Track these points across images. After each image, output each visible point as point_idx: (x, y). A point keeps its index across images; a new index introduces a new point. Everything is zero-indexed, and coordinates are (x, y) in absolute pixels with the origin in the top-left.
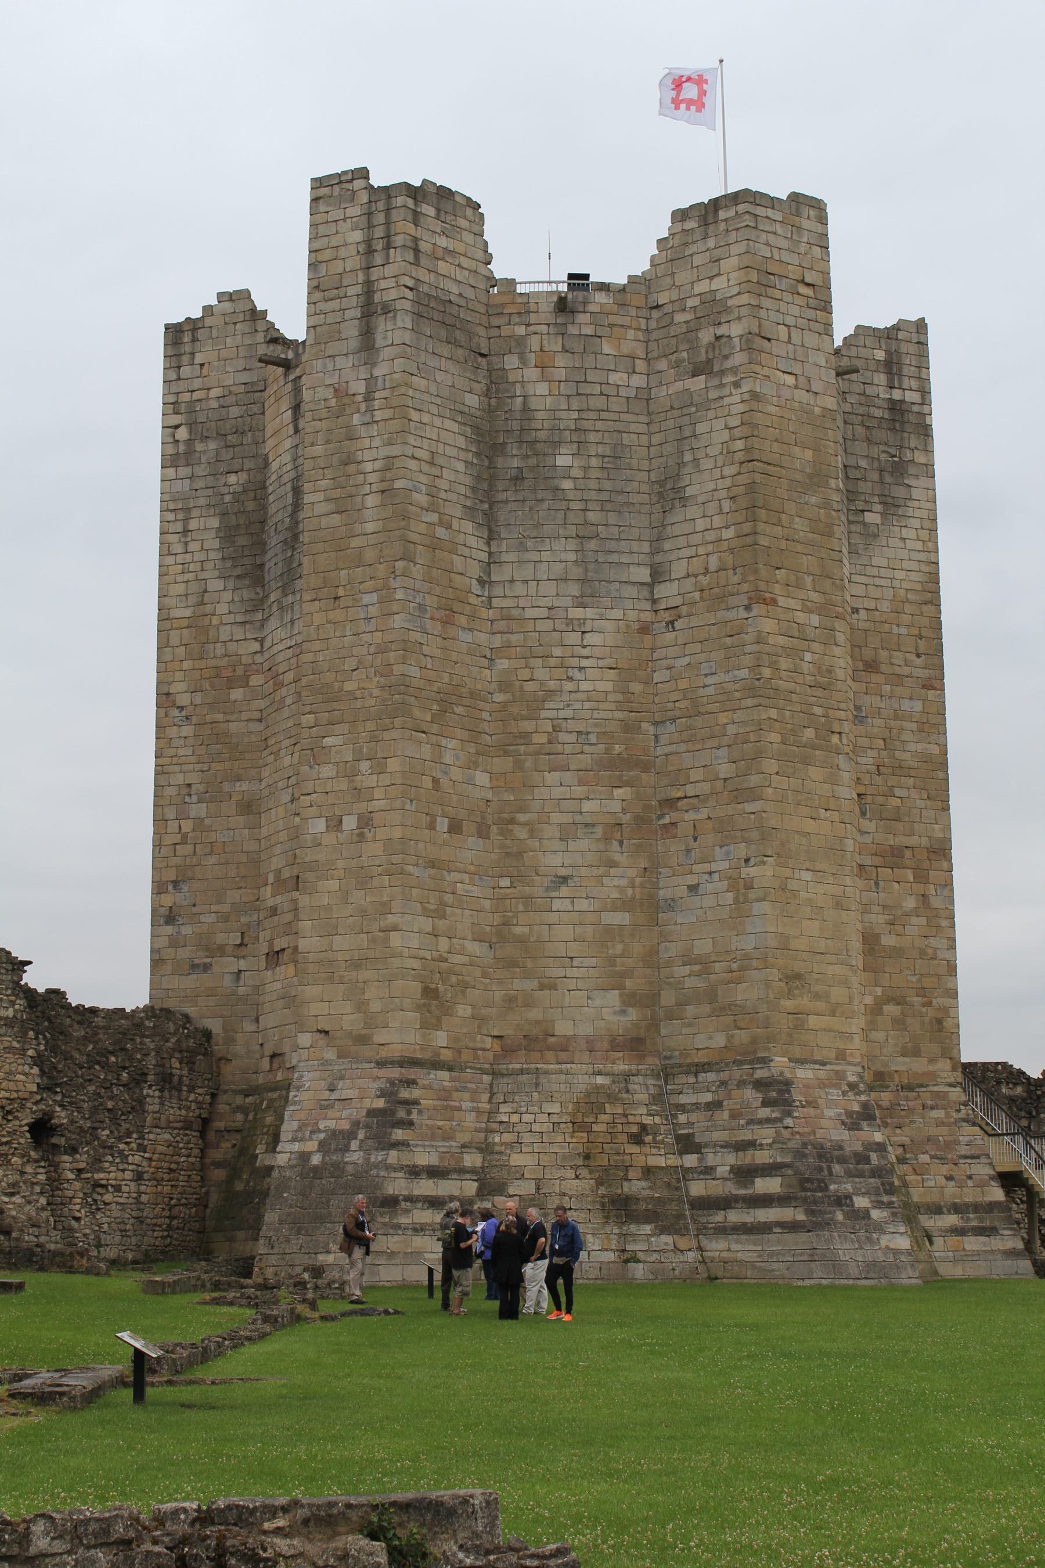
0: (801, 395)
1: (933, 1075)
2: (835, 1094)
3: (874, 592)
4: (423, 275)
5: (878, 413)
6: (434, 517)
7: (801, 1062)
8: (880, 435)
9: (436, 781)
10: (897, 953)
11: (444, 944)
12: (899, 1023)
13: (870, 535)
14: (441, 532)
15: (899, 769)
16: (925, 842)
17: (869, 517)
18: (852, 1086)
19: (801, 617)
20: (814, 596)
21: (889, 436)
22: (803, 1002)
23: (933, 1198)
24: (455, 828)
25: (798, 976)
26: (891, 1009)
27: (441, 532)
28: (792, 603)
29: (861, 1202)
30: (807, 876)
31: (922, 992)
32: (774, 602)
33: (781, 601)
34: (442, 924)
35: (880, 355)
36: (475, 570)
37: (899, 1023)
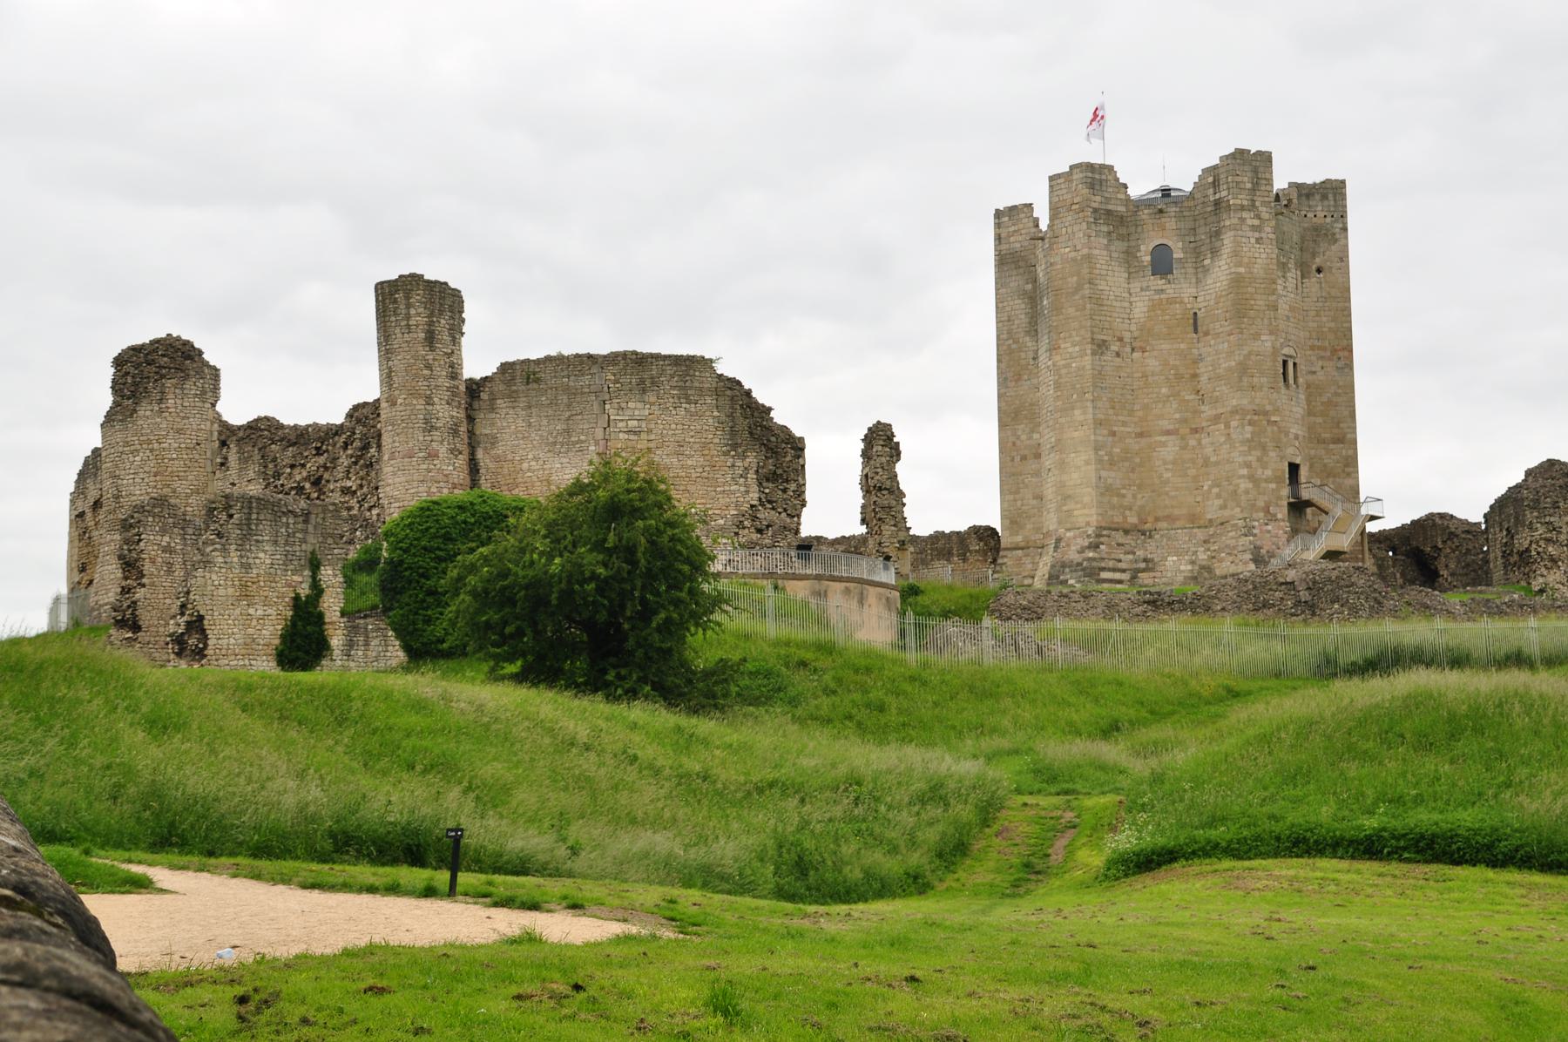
1: (1233, 517)
2: (1079, 541)
4: (1004, 247)
7: (1068, 530)
8: (1210, 219)
10: (1217, 463)
12: (1218, 496)
13: (1206, 270)
15: (1219, 378)
17: (1207, 262)
21: (1213, 218)
22: (1070, 505)
23: (1224, 572)
24: (1024, 458)
26: (1215, 490)
29: (1071, 582)
31: (1228, 479)
35: (1211, 179)
36: (1031, 355)
37: (1218, 496)
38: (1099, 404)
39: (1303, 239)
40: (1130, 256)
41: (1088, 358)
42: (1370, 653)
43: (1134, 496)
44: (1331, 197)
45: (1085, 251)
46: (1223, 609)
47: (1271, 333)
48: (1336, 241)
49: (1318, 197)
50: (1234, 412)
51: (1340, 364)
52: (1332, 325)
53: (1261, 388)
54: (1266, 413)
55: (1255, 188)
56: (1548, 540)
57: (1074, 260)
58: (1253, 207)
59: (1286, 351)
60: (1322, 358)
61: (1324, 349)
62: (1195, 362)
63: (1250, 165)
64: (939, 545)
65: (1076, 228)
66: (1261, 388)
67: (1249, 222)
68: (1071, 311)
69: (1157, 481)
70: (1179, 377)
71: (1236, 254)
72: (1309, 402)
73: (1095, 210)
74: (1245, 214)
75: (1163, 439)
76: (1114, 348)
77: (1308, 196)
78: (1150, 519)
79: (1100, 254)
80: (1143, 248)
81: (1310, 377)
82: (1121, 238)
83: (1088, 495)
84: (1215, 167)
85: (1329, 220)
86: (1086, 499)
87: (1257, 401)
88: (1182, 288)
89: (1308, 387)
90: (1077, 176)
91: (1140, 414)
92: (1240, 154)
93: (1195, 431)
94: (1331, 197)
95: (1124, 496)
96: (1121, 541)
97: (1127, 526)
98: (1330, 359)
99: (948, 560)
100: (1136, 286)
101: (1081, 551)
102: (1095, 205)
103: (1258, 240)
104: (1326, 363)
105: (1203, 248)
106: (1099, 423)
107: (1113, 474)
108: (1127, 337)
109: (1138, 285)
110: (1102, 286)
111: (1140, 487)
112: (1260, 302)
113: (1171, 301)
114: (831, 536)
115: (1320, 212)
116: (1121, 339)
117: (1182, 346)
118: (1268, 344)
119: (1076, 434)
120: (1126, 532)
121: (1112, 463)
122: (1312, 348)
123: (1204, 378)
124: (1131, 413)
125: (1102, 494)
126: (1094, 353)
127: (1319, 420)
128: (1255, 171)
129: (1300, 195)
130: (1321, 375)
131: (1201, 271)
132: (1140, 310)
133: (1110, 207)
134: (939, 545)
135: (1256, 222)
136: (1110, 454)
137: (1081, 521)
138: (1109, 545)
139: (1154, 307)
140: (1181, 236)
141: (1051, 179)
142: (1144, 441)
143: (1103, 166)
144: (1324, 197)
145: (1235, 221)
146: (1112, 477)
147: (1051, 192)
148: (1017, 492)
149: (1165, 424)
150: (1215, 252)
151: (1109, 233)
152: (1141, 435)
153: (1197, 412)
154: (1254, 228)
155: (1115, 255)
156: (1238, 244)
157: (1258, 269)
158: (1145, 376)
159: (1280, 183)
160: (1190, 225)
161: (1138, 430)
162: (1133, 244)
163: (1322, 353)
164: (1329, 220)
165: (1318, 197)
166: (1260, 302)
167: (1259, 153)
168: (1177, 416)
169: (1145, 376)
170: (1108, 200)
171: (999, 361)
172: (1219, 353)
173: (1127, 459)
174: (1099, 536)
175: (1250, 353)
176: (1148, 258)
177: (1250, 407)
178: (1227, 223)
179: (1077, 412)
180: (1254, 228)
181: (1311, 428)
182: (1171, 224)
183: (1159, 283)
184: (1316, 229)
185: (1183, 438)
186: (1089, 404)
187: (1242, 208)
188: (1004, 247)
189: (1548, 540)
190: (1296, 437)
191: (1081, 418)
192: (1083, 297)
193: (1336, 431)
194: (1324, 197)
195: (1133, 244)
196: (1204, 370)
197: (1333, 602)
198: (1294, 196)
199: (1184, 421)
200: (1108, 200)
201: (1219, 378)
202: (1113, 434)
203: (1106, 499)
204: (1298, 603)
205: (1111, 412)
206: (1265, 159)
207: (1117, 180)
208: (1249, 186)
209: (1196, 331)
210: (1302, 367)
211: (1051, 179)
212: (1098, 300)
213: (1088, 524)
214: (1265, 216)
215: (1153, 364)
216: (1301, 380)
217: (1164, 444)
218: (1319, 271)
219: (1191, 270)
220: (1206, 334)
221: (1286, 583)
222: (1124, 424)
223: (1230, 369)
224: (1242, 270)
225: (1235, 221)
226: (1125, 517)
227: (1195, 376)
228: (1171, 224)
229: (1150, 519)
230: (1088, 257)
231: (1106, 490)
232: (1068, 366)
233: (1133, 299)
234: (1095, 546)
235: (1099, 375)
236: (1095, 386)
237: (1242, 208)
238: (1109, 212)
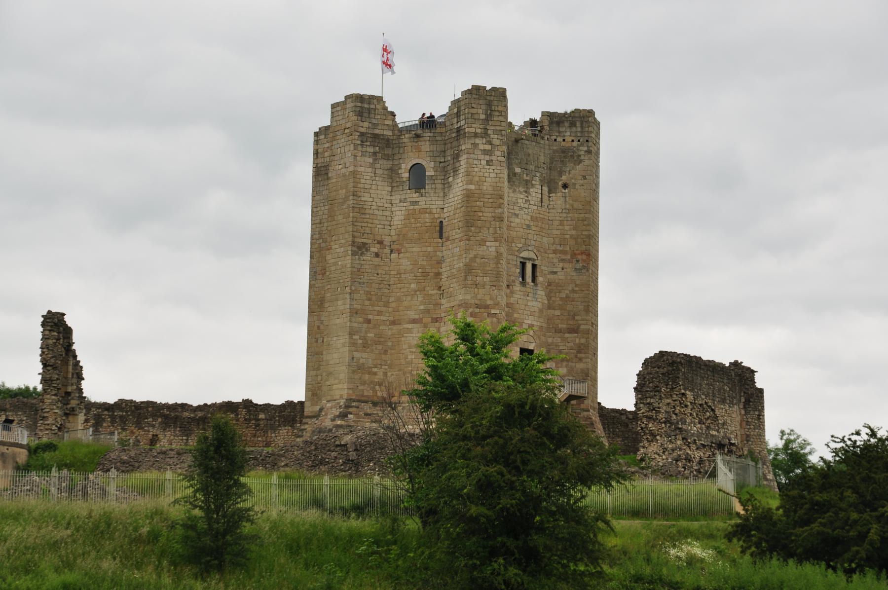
0: (344, 171)
3: (450, 209)
4: (320, 160)
5: (454, 135)
6: (321, 241)
7: (328, 401)
9: (318, 327)
11: (319, 378)
14: (323, 245)
15: (453, 276)
16: (458, 302)
17: (451, 179)
18: (340, 407)
19: (338, 250)
20: (343, 241)
21: (455, 143)
25: (331, 373)
27: (323, 245)
28: (337, 246)
30: (335, 339)
32: (331, 248)
33: (333, 247)
34: (319, 372)
35: (455, 111)
38: (356, 296)
39: (552, 159)
40: (393, 172)
41: (349, 257)
42: (358, 501)
43: (385, 374)
44: (578, 124)
45: (351, 169)
46: (286, 465)
47: (496, 240)
48: (580, 161)
49: (567, 124)
50: (460, 306)
51: (578, 266)
52: (574, 232)
53: (483, 286)
54: (487, 307)
55: (489, 118)
56: (650, 418)
57: (344, 175)
58: (485, 134)
59: (525, 254)
60: (563, 260)
61: (564, 252)
62: (440, 262)
63: (486, 102)
64: (286, 413)
65: (347, 148)
66: (483, 286)
67: (481, 147)
68: (340, 217)
69: (403, 362)
70: (425, 275)
71: (468, 174)
72: (549, 297)
73: (362, 134)
74: (478, 141)
75: (410, 326)
76: (374, 249)
77: (559, 123)
78: (397, 394)
79: (366, 172)
80: (403, 166)
81: (551, 277)
82: (387, 157)
83: (343, 372)
84: (458, 100)
85: (575, 144)
86: (342, 376)
87: (479, 297)
88: (431, 201)
89: (550, 284)
90: (350, 105)
91: (393, 305)
92: (476, 92)
93: (436, 320)
94: (578, 124)
95: (375, 374)
96: (369, 411)
97: (375, 399)
98: (570, 262)
99: (292, 426)
100: (396, 198)
101: (333, 420)
102: (363, 130)
103: (489, 163)
104: (566, 265)
105: (447, 170)
106: (354, 312)
107: (365, 355)
108: (387, 240)
109: (398, 197)
110: (366, 197)
111: (390, 366)
112: (488, 214)
113: (423, 211)
114: (195, 404)
115: (568, 137)
116: (380, 242)
117: (429, 249)
118: (493, 249)
119: (338, 321)
120: (375, 404)
121: (365, 346)
122: (555, 252)
123: (444, 276)
124: (387, 304)
125: (354, 372)
126: (354, 254)
127: (558, 313)
128: (489, 104)
129: (551, 123)
130: (561, 276)
131: (447, 186)
132: (398, 218)
133: (377, 132)
134: (286, 413)
135: (488, 147)
136: (364, 338)
137: (337, 393)
138: (357, 415)
139: (407, 217)
140: (434, 157)
141: (334, 106)
142: (396, 328)
143: (372, 98)
144: (573, 124)
145: (469, 146)
146: (365, 357)
147: (332, 117)
148: (318, 369)
149: (412, 314)
150: (455, 171)
151: (375, 154)
152: (393, 323)
153: (438, 305)
154: (485, 152)
155: (378, 171)
156: (470, 165)
157: (487, 187)
158: (399, 274)
159: (518, 114)
160: (442, 148)
161: (392, 319)
162: (396, 162)
163: (563, 257)
164: (575, 144)
165: (567, 124)
166: (488, 214)
167: (494, 89)
168: (422, 307)
169: (399, 274)
170: (375, 126)
171: (312, 257)
172: (454, 255)
173: (379, 343)
174: (347, 407)
175: (475, 257)
176: (407, 175)
177: (473, 302)
178: (463, 147)
179: (340, 303)
180: (485, 152)
181: (549, 320)
182: (426, 146)
183: (415, 196)
184: (564, 151)
185: (425, 326)
186: (348, 296)
187: (476, 135)
188: (320, 160)
189: (650, 418)
190: (531, 326)
191: (342, 308)
192: (348, 207)
193: (571, 322)
194: (573, 124)
195: (396, 162)
196: (444, 269)
197: (370, 461)
198: (546, 123)
199: (428, 311)
200: (375, 126)
201: (453, 276)
202: (369, 321)
203: (357, 377)
204: (348, 461)
205: (367, 303)
206: (500, 94)
207: (386, 108)
208: (483, 117)
209: (441, 237)
210: (543, 268)
211: (334, 106)
212: (360, 210)
213: (341, 397)
214: (496, 142)
215: (406, 264)
216: (540, 279)
217: (410, 331)
218: (565, 186)
219: (440, 186)
220: (448, 240)
221: (341, 445)
222: (379, 313)
223: (459, 270)
224: (472, 187)
225: (469, 146)
226: (375, 391)
227: (438, 274)
228: (426, 146)
229: (397, 394)
230: (354, 174)
231: (358, 369)
232: (335, 264)
233: (391, 208)
234: (343, 416)
235: (357, 273)
236: (353, 281)
237: (476, 135)
238: (376, 136)
